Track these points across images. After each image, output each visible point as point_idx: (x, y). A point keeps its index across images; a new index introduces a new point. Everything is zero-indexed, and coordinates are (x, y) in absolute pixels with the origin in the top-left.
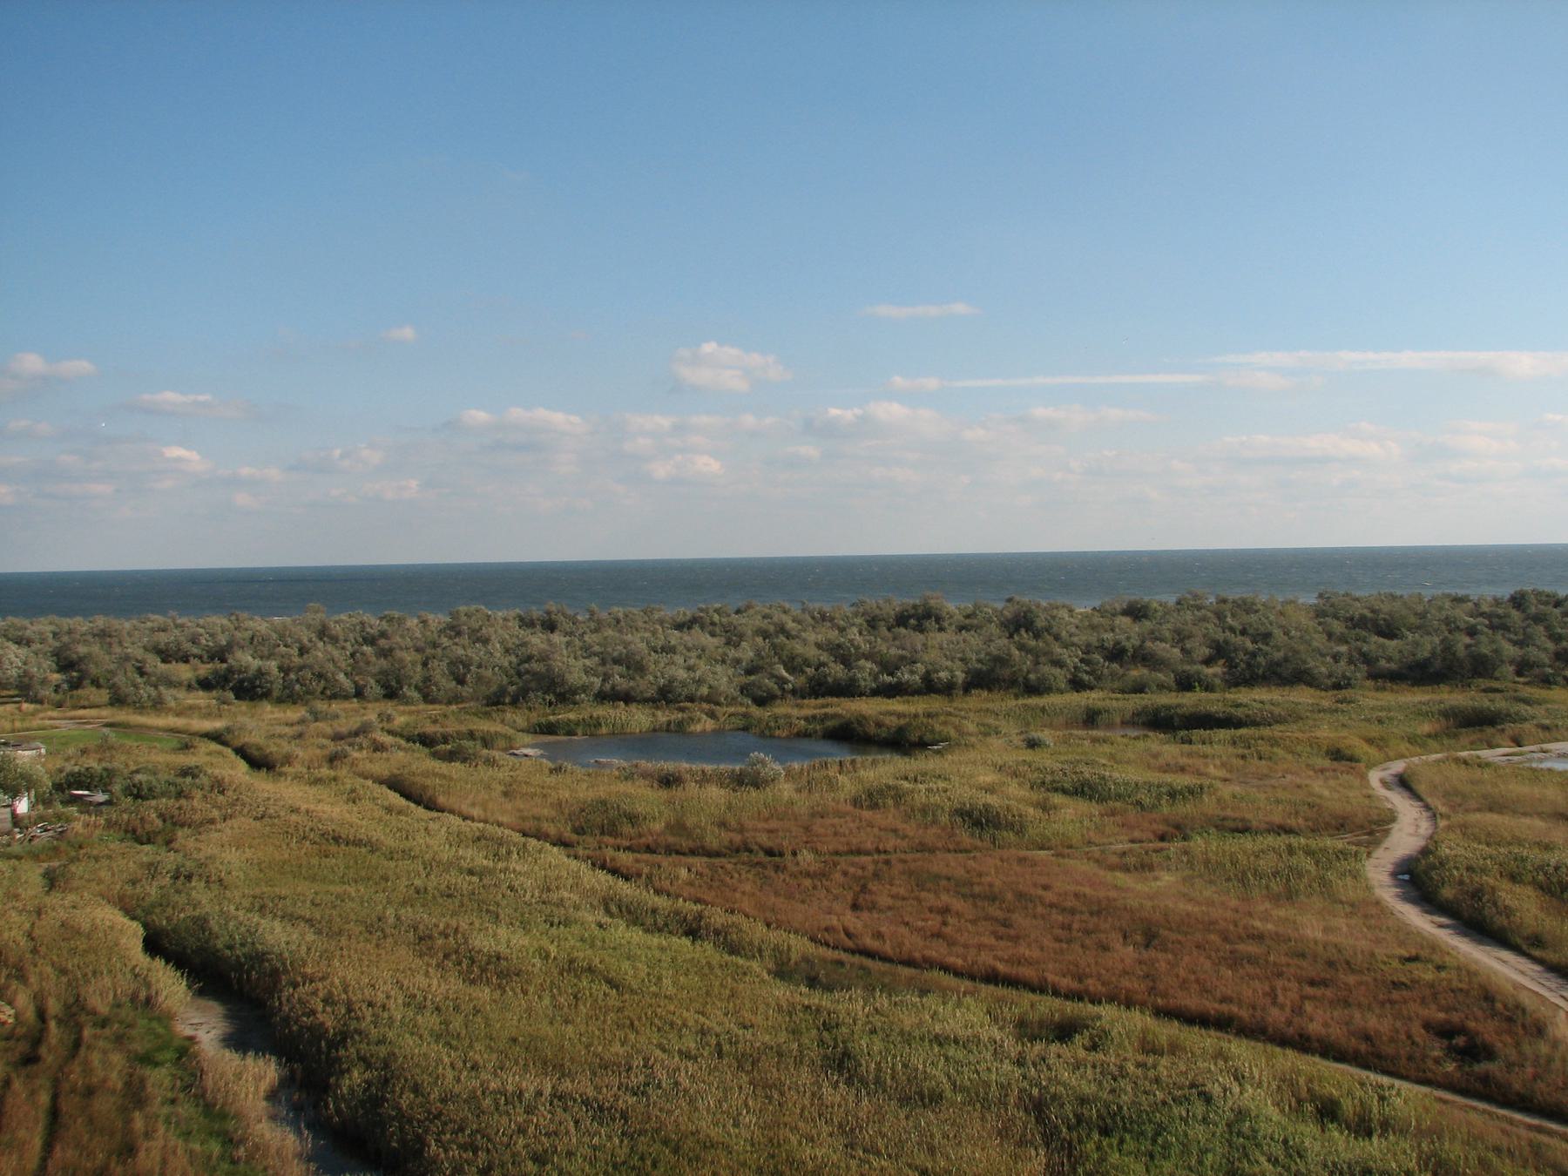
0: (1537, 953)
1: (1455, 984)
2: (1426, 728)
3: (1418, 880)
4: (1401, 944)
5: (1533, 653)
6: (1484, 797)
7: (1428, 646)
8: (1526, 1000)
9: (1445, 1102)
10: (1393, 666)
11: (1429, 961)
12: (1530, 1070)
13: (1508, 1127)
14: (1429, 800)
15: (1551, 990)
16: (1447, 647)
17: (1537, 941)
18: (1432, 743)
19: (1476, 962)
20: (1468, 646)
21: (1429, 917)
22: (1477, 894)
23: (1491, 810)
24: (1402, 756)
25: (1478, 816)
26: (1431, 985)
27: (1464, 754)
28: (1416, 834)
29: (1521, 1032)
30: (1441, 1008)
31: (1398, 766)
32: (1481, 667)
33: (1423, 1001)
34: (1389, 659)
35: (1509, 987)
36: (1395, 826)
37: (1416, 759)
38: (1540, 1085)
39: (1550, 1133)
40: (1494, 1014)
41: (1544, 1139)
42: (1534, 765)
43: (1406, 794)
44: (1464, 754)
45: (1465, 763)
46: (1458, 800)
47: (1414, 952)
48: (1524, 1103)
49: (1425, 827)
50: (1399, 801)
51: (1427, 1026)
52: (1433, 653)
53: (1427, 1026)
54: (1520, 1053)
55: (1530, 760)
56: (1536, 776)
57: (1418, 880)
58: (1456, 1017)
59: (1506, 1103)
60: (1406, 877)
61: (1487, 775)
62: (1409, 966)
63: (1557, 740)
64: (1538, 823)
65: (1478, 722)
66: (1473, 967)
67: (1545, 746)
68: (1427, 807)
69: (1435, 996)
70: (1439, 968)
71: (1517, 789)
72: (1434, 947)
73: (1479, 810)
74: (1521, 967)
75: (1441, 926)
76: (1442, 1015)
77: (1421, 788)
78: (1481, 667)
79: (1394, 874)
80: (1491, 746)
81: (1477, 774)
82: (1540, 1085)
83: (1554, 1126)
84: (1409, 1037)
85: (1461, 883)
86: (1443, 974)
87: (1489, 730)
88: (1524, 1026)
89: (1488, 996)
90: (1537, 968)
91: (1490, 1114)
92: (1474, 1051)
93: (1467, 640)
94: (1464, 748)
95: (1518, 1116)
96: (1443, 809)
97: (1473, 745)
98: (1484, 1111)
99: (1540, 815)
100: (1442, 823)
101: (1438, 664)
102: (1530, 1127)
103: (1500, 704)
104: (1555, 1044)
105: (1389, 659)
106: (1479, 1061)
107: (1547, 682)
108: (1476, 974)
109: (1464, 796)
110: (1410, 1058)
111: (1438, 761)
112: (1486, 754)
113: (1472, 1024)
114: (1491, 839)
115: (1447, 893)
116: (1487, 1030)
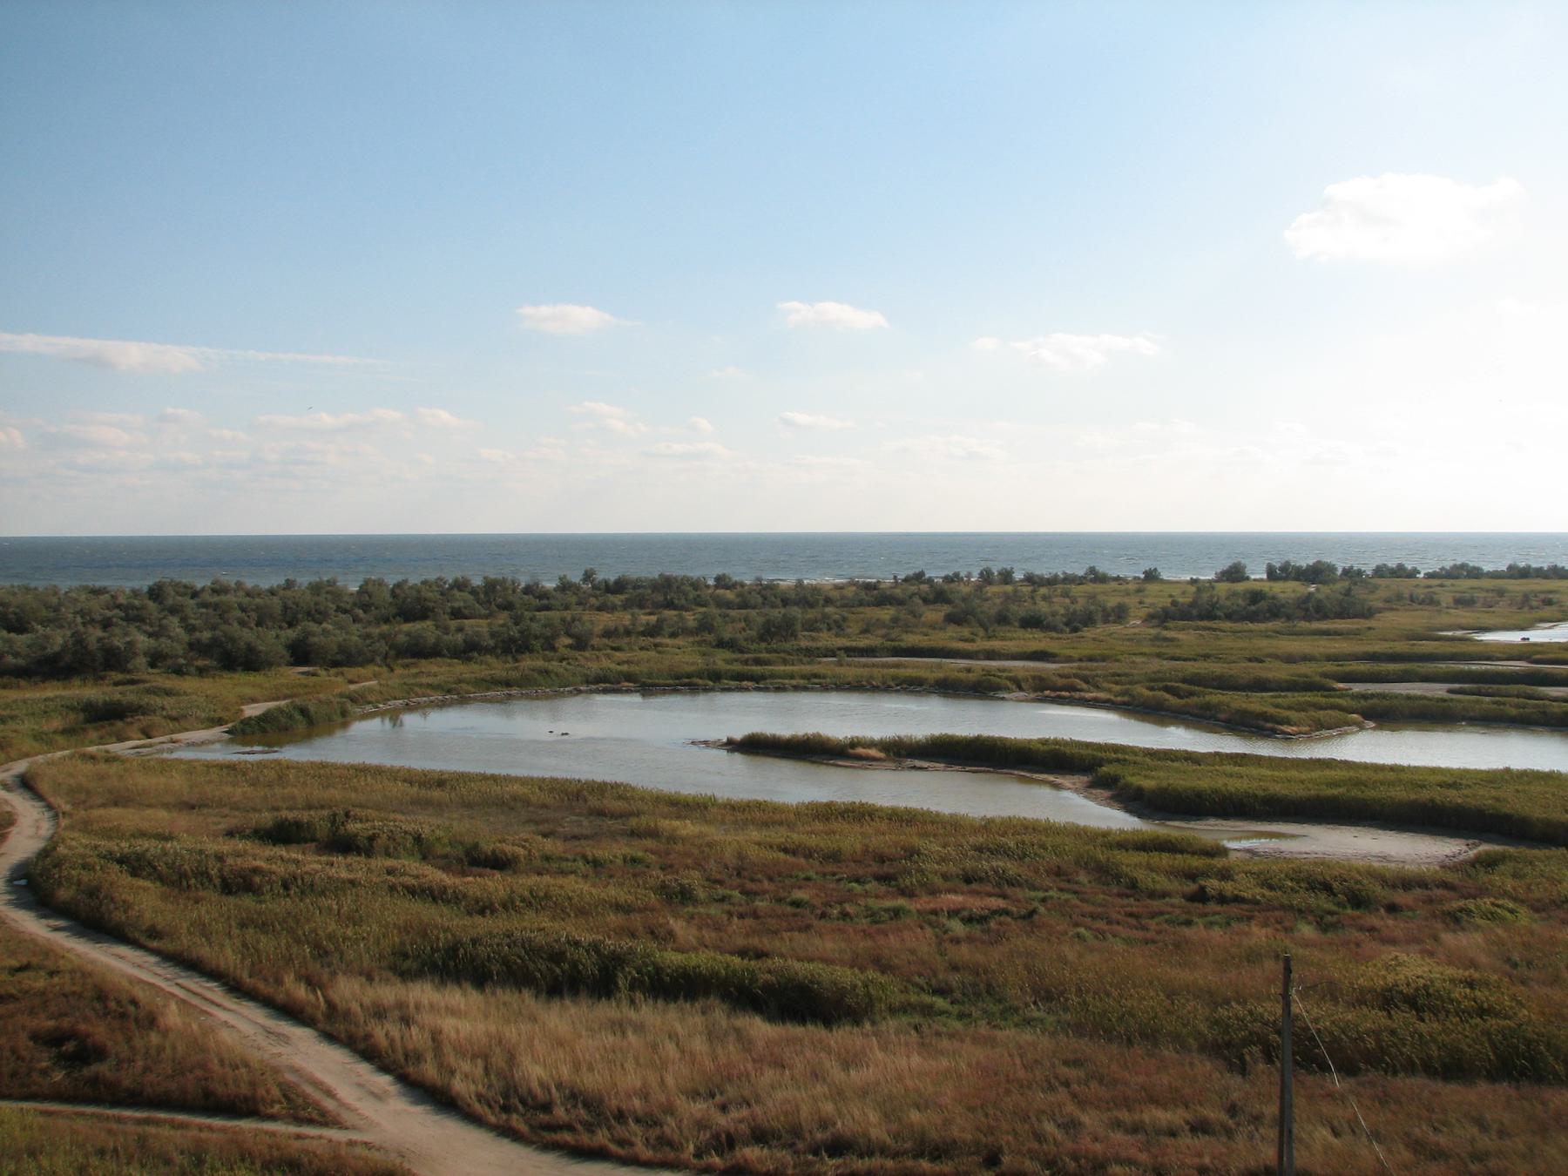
0: (155, 944)
1: (68, 988)
2: (57, 723)
3: (35, 886)
4: (13, 954)
5: (164, 644)
6: (110, 792)
7: (58, 639)
8: (140, 994)
9: (49, 1114)
10: (21, 662)
11: (41, 967)
12: (140, 1063)
13: (115, 1126)
14: (52, 799)
15: (167, 979)
16: (79, 641)
17: (154, 933)
18: (61, 740)
19: (93, 962)
20: (100, 640)
21: (44, 921)
22: (93, 892)
23: (116, 804)
24: (27, 755)
25: (102, 811)
26: (43, 993)
27: (93, 749)
28: (36, 836)
29: (133, 1026)
30: (52, 1017)
31: (21, 766)
32: (112, 661)
33: (32, 1012)
34: (16, 655)
35: (125, 983)
36: (14, 830)
37: (40, 758)
38: (151, 1077)
39: (157, 1123)
40: (106, 1013)
41: (152, 1130)
42: (165, 756)
43: (28, 795)
44: (93, 749)
45: (92, 758)
46: (83, 797)
47: (25, 961)
48: (133, 1098)
49: (46, 828)
50: (20, 803)
51: (35, 1037)
52: (64, 647)
53: (35, 1037)
54: (132, 1048)
55: (162, 751)
56: (165, 767)
57: (35, 886)
58: (66, 1023)
59: (116, 1103)
60: (23, 882)
61: (114, 769)
62: (20, 976)
63: (187, 730)
64: (163, 814)
65: (107, 716)
66: (89, 967)
67: (175, 736)
68: (50, 807)
69: (45, 1003)
70: (52, 974)
71: (143, 781)
72: (48, 952)
73: (104, 805)
74: (140, 961)
75: (57, 929)
76: (51, 1023)
77: (44, 787)
78: (112, 661)
79: (10, 881)
80: (121, 739)
81: (103, 767)
82: (151, 1077)
83: (162, 1115)
84: (14, 1051)
85: (79, 883)
86: (56, 980)
87: (119, 724)
88: (137, 1020)
89: (101, 995)
90: (153, 959)
91: (99, 1117)
92: (82, 1053)
93: (99, 633)
94: (92, 743)
95: (128, 1113)
96: (67, 808)
97: (102, 741)
98: (93, 1115)
99: (166, 806)
100: (64, 822)
101: (68, 658)
102: (139, 1122)
103: (129, 695)
104: (165, 1033)
105: (16, 655)
106: (89, 1064)
107: (179, 672)
108: (90, 974)
109: (88, 792)
110: (14, 1075)
111: (64, 758)
112: (116, 748)
113: (83, 1027)
114: (108, 833)
115: (64, 894)
116: (99, 1031)
